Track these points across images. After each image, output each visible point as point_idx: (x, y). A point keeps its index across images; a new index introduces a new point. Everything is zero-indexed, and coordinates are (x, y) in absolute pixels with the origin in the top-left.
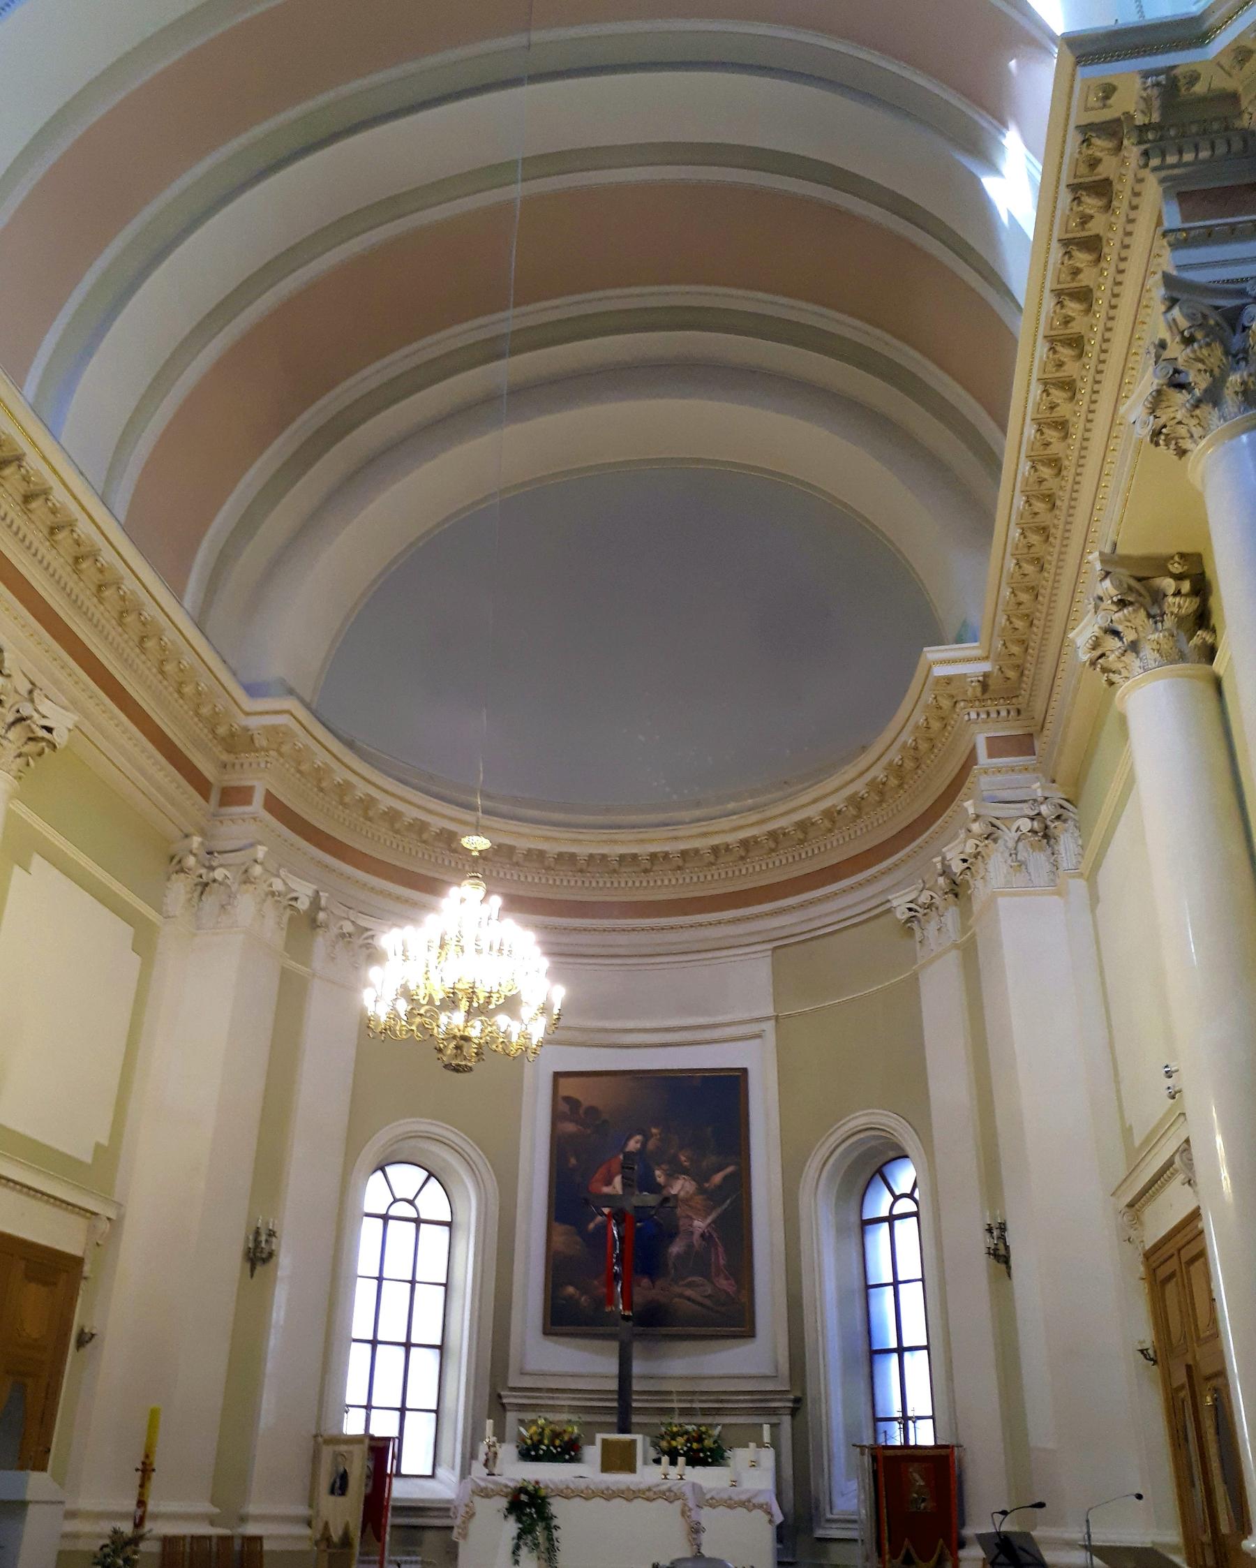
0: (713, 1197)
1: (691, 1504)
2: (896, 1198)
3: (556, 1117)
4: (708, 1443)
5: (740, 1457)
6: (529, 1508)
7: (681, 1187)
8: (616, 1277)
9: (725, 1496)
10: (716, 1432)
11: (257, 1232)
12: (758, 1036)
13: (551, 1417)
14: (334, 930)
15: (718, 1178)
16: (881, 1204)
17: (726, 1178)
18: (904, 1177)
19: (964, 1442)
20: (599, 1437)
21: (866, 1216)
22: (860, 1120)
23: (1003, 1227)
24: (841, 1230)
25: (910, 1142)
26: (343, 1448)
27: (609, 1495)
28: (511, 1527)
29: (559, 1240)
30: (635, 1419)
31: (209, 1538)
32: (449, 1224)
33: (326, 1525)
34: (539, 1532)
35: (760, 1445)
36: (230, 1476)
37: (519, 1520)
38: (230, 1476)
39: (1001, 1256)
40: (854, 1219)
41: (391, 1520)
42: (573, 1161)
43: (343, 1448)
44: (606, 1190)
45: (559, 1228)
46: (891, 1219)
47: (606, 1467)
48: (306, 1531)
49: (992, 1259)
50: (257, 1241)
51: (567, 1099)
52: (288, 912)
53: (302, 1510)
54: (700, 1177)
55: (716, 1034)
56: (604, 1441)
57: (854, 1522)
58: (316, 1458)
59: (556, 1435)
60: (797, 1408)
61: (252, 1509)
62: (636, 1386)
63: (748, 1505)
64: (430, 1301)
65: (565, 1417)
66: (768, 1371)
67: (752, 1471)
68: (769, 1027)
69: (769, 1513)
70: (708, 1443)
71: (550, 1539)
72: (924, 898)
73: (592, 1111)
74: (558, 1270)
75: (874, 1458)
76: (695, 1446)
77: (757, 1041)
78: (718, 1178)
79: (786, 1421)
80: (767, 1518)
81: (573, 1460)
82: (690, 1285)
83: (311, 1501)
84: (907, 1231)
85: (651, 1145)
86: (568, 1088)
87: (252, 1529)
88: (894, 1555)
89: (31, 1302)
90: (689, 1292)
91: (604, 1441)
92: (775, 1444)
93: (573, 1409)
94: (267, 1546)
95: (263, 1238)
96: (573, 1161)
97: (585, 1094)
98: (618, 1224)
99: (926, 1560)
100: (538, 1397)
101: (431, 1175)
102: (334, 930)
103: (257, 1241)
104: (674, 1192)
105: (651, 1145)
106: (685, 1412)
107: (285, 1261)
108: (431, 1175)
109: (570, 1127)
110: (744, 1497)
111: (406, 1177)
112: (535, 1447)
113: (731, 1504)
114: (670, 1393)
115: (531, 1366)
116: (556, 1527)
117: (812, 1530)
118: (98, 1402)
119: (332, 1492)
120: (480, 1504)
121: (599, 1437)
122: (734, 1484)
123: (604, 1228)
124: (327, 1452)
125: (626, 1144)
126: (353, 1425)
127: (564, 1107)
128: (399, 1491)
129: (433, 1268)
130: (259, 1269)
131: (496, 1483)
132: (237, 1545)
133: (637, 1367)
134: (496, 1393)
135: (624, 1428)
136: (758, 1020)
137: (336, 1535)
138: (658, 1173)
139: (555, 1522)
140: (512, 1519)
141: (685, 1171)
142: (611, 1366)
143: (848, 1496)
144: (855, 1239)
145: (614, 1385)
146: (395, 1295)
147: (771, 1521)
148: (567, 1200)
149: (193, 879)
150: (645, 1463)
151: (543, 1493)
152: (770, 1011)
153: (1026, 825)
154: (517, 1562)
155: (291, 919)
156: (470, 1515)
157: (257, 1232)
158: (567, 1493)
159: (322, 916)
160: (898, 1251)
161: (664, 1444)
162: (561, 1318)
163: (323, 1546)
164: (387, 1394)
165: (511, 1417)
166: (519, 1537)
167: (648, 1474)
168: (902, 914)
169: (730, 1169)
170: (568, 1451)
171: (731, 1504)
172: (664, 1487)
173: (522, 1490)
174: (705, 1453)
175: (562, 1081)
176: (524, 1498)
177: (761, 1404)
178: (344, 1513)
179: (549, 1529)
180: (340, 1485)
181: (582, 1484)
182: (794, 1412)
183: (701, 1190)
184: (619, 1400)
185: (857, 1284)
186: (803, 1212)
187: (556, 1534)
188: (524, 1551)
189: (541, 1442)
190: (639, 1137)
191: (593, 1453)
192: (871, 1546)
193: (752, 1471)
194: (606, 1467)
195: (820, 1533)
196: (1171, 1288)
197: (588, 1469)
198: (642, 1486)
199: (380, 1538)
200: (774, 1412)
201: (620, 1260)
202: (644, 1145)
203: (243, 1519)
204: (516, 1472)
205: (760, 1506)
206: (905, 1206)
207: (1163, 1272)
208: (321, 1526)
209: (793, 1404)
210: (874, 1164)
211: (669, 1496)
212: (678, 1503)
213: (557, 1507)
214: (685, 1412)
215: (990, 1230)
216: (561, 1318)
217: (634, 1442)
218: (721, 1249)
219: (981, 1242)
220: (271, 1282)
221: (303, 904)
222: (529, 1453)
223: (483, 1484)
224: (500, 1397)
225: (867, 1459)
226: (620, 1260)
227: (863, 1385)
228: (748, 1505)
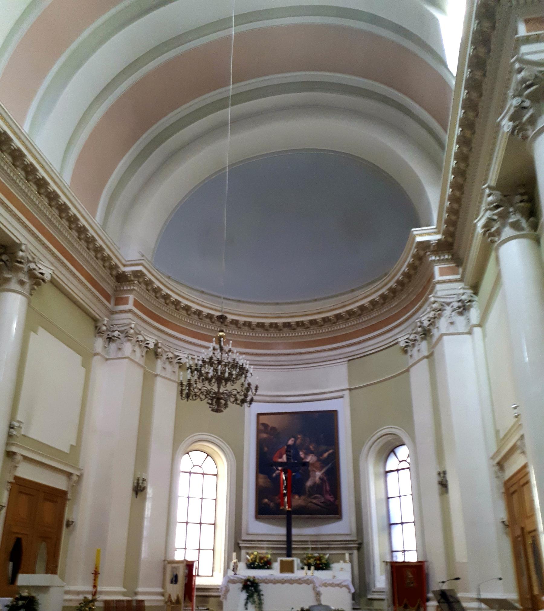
0: (324, 462)
1: (317, 585)
3: (259, 432)
4: (324, 561)
5: (336, 566)
6: (251, 588)
7: (310, 459)
8: (284, 495)
9: (331, 582)
10: (327, 556)
11: (138, 480)
12: (342, 397)
13: (260, 551)
14: (165, 357)
15: (326, 455)
17: (329, 455)
18: (403, 452)
19: (429, 558)
20: (279, 559)
21: (388, 469)
23: (445, 473)
24: (376, 475)
25: (405, 438)
26: (176, 565)
27: (283, 582)
28: (244, 595)
29: (261, 481)
30: (294, 552)
31: (123, 601)
32: (216, 475)
33: (170, 596)
34: (255, 597)
35: (345, 561)
36: (131, 576)
37: (247, 592)
38: (131, 576)
39: (443, 485)
40: (382, 470)
41: (195, 593)
42: (266, 449)
43: (176, 565)
44: (280, 460)
45: (261, 476)
47: (282, 570)
48: (160, 598)
49: (440, 486)
50: (138, 483)
51: (263, 424)
52: (146, 349)
53: (160, 590)
54: (319, 455)
56: (282, 562)
57: (383, 592)
58: (164, 568)
59: (261, 558)
61: (140, 589)
62: (294, 539)
63: (340, 585)
64: (209, 505)
65: (264, 551)
66: (347, 532)
67: (342, 571)
68: (347, 393)
69: (348, 588)
70: (324, 561)
71: (260, 599)
73: (273, 428)
74: (261, 493)
75: (392, 567)
76: (318, 562)
77: (341, 399)
78: (326, 455)
79: (355, 552)
80: (347, 590)
81: (268, 568)
82: (316, 498)
83: (163, 587)
85: (298, 441)
86: (263, 420)
87: (140, 598)
88: (400, 605)
89: (48, 507)
90: (314, 501)
91: (282, 562)
92: (351, 561)
93: (268, 548)
94: (146, 604)
95: (141, 481)
96: (266, 449)
97: (270, 422)
98: (285, 474)
99: (413, 606)
100: (253, 543)
101: (208, 455)
102: (165, 357)
103: (138, 483)
104: (308, 460)
105: (298, 441)
106: (313, 549)
107: (150, 491)
108: (208, 455)
109: (265, 436)
110: (338, 582)
111: (197, 457)
112: (253, 562)
113: (332, 585)
114: (307, 541)
115: (251, 531)
116: (263, 595)
117: (365, 596)
118: (76, 547)
119: (172, 582)
120: (231, 586)
121: (279, 559)
122: (334, 577)
123: (279, 475)
124: (169, 567)
125: (287, 442)
126: (179, 556)
127: (261, 427)
128: (199, 582)
129: (210, 493)
130: (139, 494)
131: (238, 578)
132: (134, 604)
133: (294, 531)
134: (237, 543)
135: (289, 555)
137: (174, 598)
138: (301, 453)
139: (262, 593)
140: (244, 592)
141: (312, 452)
142: (283, 531)
143: (381, 581)
145: (284, 538)
146: (195, 504)
147: (350, 592)
148: (264, 465)
149: (105, 336)
150: (298, 569)
151: (257, 581)
152: (347, 386)
154: (246, 609)
155: (147, 352)
156: (227, 591)
157: (138, 480)
158: (266, 581)
159: (159, 350)
160: (400, 484)
161: (305, 562)
162: (263, 511)
163: (169, 603)
164: (193, 544)
165: (243, 552)
166: (247, 599)
167: (299, 574)
168: (402, 344)
169: (331, 451)
170: (266, 564)
171: (332, 585)
172: (305, 579)
173: (248, 580)
174: (322, 565)
175: (261, 417)
176: (249, 583)
177: (345, 545)
178: (176, 591)
179: (259, 595)
180: (175, 580)
181: (272, 578)
183: (319, 460)
184: (287, 545)
185: (383, 497)
186: (361, 468)
187: (262, 597)
188: (249, 605)
189: (255, 561)
190: (293, 439)
191: (276, 565)
192: (390, 601)
193: (342, 571)
194: (282, 570)
195: (370, 597)
197: (275, 572)
198: (297, 578)
199: (191, 600)
201: (286, 488)
202: (295, 442)
203: (136, 594)
204: (245, 573)
205: (345, 586)
206: (405, 465)
208: (167, 596)
209: (358, 545)
211: (308, 582)
212: (311, 585)
213: (262, 587)
214: (313, 549)
215: (439, 474)
216: (263, 511)
217: (293, 561)
218: (327, 484)
219: (435, 480)
220: (144, 499)
221: (151, 346)
222: (251, 566)
223: (232, 578)
224: (238, 544)
225: (389, 567)
226: (286, 488)
227: (386, 537)
228: (340, 585)
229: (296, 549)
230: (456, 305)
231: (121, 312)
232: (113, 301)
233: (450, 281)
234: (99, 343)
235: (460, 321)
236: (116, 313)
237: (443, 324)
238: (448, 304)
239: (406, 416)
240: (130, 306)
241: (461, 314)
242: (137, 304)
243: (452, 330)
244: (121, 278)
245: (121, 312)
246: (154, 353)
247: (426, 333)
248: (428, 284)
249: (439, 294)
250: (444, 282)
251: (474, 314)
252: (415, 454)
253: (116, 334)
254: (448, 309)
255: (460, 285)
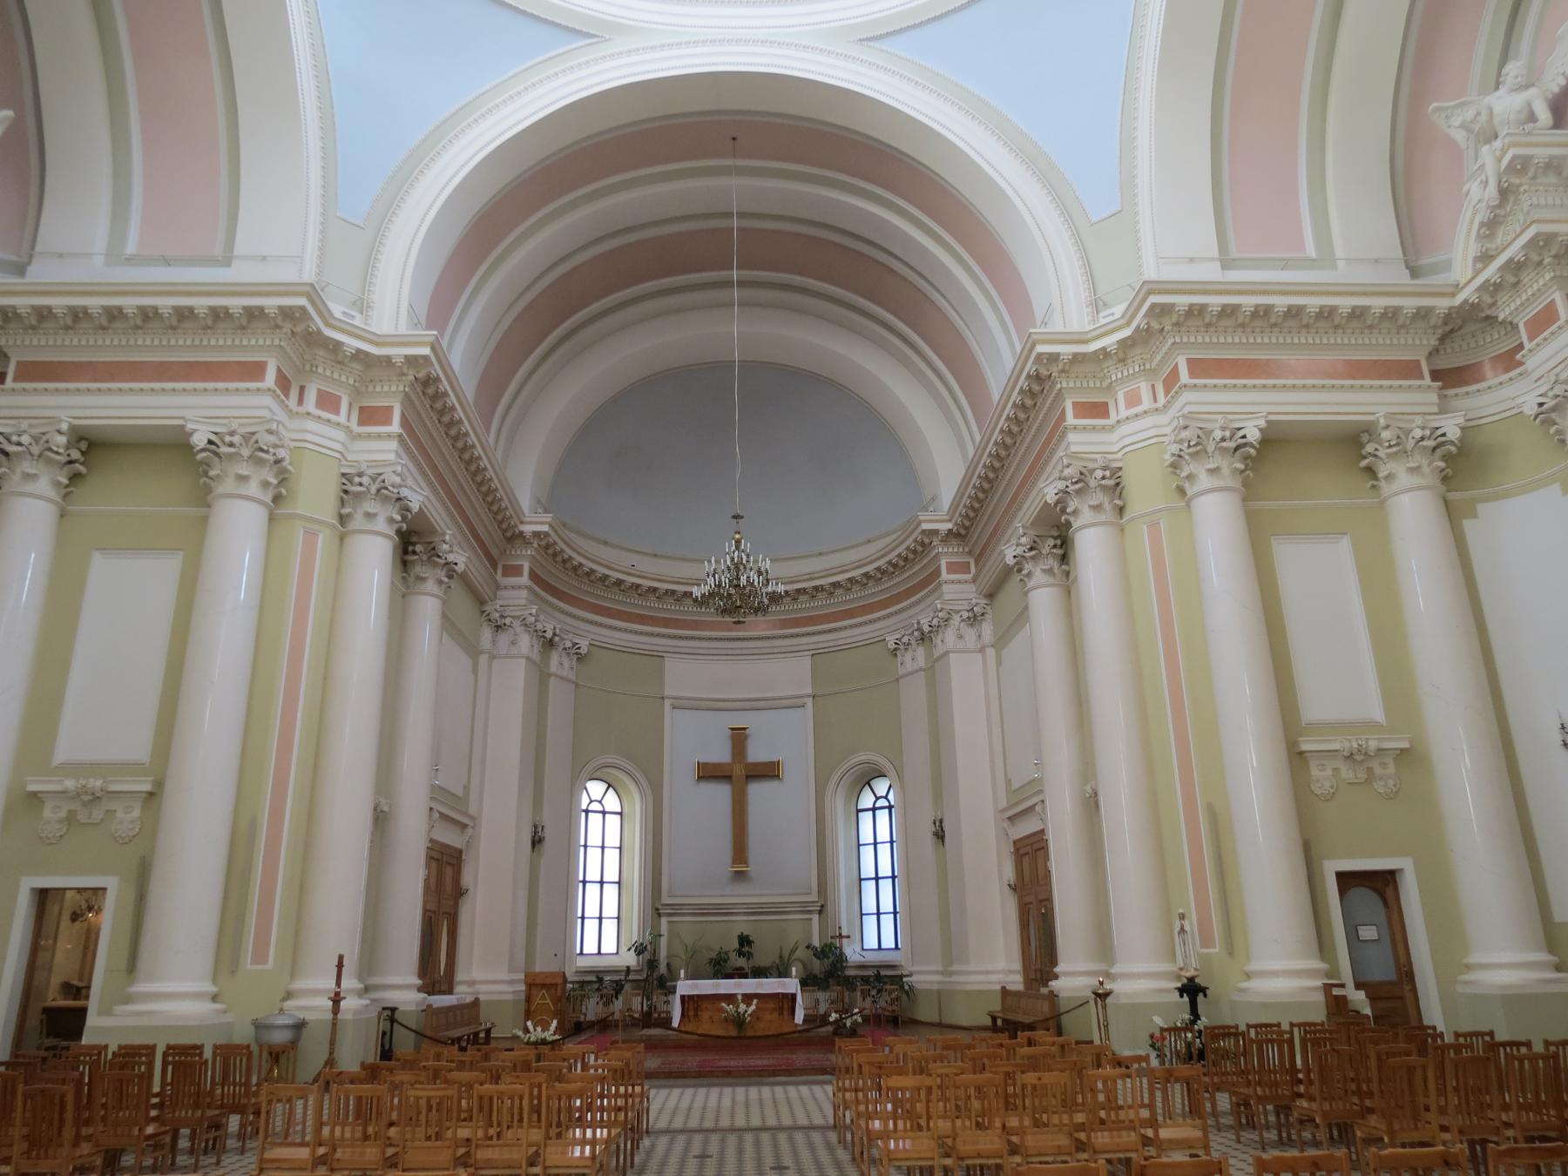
2: (877, 798)
18: (881, 786)
46: (874, 809)
68: (809, 701)
79: (816, 917)
152: (809, 690)
160: (876, 828)
182: (820, 912)
196: (1026, 860)
200: (810, 912)
207: (1022, 851)
230: (965, 615)
232: (500, 571)
234: (487, 633)
235: (970, 634)
237: (950, 636)
238: (957, 612)
240: (525, 579)
242: (534, 576)
243: (960, 645)
246: (550, 644)
247: (924, 638)
248: (931, 579)
249: (946, 597)
251: (987, 629)
253: (508, 621)
254: (957, 618)
255: (972, 588)
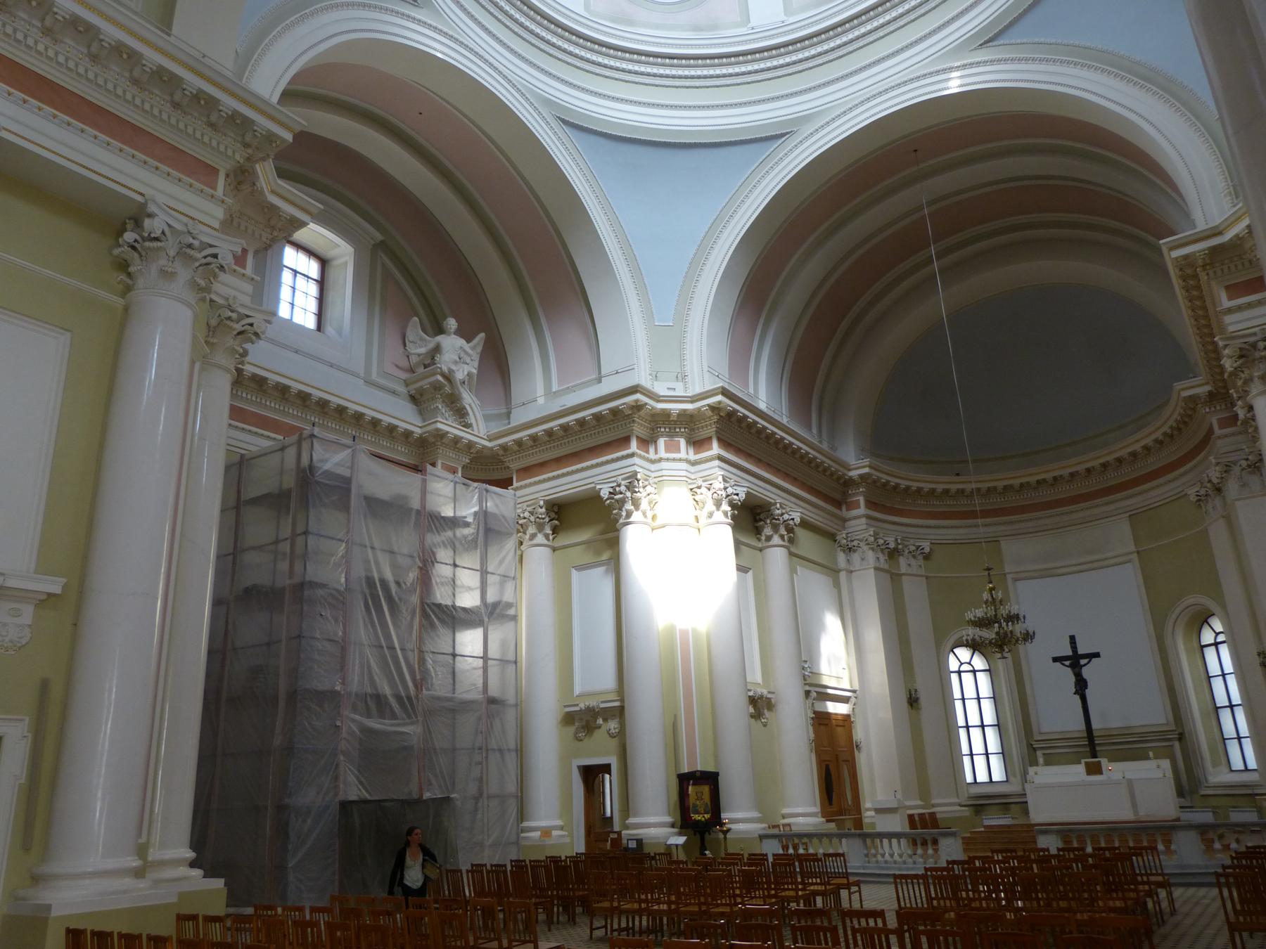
12: (1129, 562)
16: (1207, 637)
22: (1190, 600)
55: (1106, 563)
60: (1181, 737)
66: (1164, 721)
72: (1203, 492)
79: (1177, 744)
84: (1224, 650)
135: (1094, 756)
136: (1240, 308)
144: (1198, 655)
153: (1244, 463)
160: (1220, 661)
168: (1193, 498)
210: (1203, 619)
217: (1099, 763)
227: (1214, 723)
229: (1100, 745)
230: (1244, 463)
231: (855, 518)
233: (1233, 434)
236: (850, 520)
238: (1235, 463)
239: (1214, 588)
240: (862, 510)
241: (1252, 473)
242: (870, 504)
244: (849, 483)
245: (855, 518)
250: (1226, 436)
252: (1230, 630)
253: (855, 543)
254: (1237, 469)
